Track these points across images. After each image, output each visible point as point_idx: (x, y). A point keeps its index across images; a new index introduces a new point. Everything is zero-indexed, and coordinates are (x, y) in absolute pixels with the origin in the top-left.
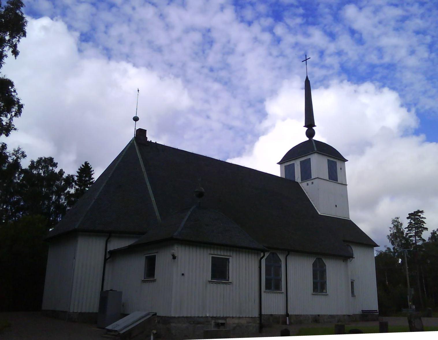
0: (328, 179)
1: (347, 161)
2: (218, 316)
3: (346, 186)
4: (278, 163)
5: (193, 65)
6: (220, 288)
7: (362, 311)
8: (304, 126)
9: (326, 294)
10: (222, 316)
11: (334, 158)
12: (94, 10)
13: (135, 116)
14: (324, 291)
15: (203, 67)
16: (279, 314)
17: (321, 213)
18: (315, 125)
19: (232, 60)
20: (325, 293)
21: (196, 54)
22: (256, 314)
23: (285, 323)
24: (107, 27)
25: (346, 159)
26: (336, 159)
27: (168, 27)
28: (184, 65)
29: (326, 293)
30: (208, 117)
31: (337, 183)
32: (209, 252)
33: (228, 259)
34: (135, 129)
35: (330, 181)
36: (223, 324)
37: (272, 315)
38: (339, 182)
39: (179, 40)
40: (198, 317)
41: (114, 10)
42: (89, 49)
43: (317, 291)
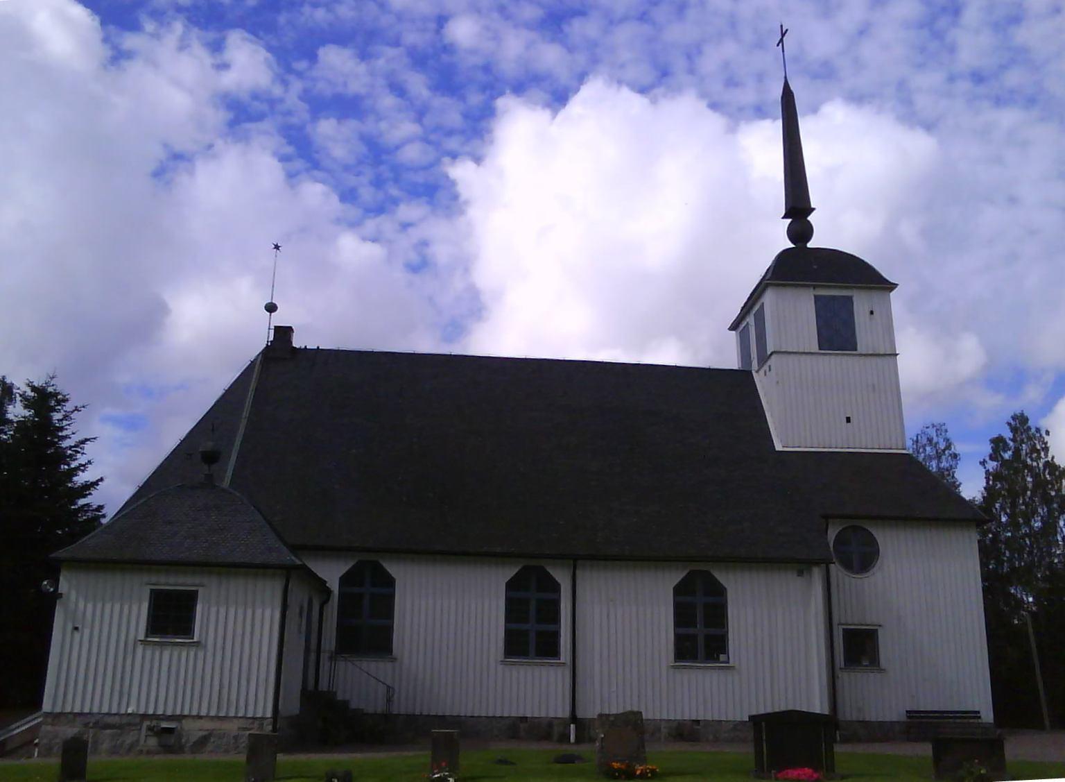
0: (815, 348)
2: (160, 712)
7: (907, 711)
8: (783, 218)
9: (727, 665)
10: (169, 713)
11: (841, 287)
12: (646, 29)
13: (270, 301)
16: (552, 715)
17: (784, 447)
19: (1022, 35)
20: (722, 663)
23: (564, 738)
29: (728, 663)
30: (1013, 200)
31: (861, 355)
34: (269, 329)
37: (524, 719)
38: (861, 348)
43: (694, 658)
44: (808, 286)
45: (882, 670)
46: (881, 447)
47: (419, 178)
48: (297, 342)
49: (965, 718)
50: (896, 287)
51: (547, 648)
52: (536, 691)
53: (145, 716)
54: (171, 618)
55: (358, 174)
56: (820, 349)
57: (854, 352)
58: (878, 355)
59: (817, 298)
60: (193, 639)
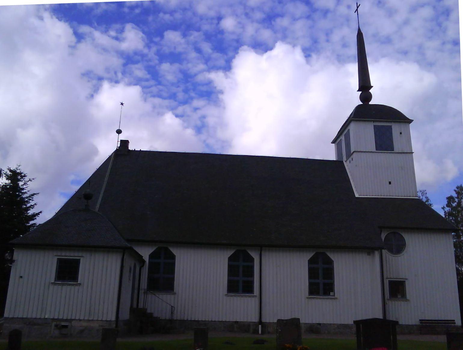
0: (374, 150)
1: (410, 121)
2: (61, 317)
3: (409, 155)
4: (332, 143)
5: (432, 45)
6: (66, 290)
7: (420, 320)
8: (358, 91)
10: (65, 318)
11: (386, 122)
14: (332, 294)
15: (444, 43)
16: (249, 321)
17: (359, 195)
18: (372, 85)
21: (432, 31)
22: (114, 319)
23: (256, 332)
24: (327, 35)
25: (411, 120)
26: (391, 122)
27: (391, 13)
28: (420, 47)
29: (334, 296)
32: (55, 253)
33: (79, 260)
35: (378, 152)
36: (66, 327)
37: (236, 322)
38: (396, 150)
39: (406, 22)
40: (36, 318)
41: (329, 15)
42: (317, 61)
43: (318, 293)
44: (371, 121)
45: (407, 300)
46: (406, 196)
47: (204, 89)
48: (131, 147)
49: (447, 323)
50: (412, 122)
51: (248, 289)
52: (242, 309)
53: (53, 319)
54: (67, 272)
55: (178, 87)
56: (376, 150)
57: (393, 152)
58: (404, 153)
59: (374, 126)
60: (77, 282)
